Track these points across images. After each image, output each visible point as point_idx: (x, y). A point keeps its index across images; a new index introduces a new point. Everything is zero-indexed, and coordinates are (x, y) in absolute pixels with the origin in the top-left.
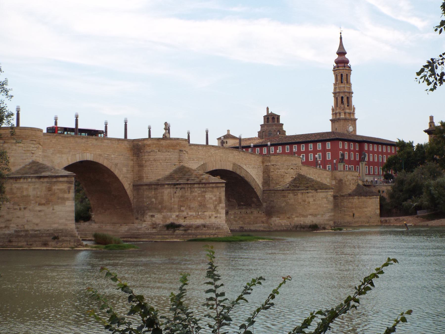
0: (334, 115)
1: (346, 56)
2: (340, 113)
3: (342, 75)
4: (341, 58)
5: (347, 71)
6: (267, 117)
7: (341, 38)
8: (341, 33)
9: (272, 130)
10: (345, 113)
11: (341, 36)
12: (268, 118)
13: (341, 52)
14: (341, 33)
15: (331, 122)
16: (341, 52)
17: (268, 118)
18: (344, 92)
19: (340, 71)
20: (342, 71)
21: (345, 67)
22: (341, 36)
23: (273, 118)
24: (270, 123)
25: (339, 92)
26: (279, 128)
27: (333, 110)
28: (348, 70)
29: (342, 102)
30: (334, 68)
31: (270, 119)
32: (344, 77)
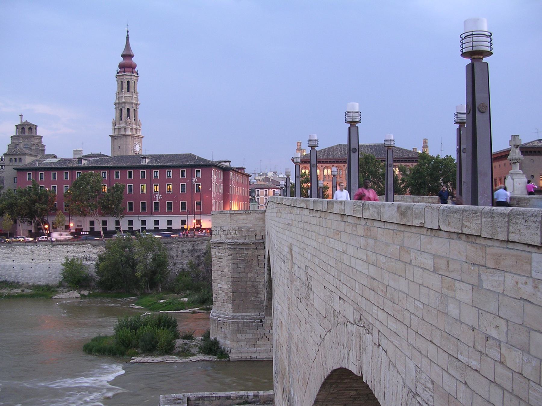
0: (117, 130)
1: (134, 60)
2: (125, 128)
3: (128, 82)
4: (127, 61)
5: (135, 78)
6: (21, 127)
7: (128, 38)
8: (128, 32)
9: (29, 144)
10: (132, 129)
11: (128, 35)
12: (23, 128)
13: (127, 55)
14: (128, 32)
15: (110, 138)
16: (127, 55)
17: (23, 128)
18: (132, 103)
19: (127, 77)
20: (129, 77)
21: (133, 73)
22: (128, 35)
23: (30, 129)
24: (27, 134)
25: (125, 103)
26: (37, 141)
27: (114, 124)
28: (136, 76)
29: (128, 115)
30: (118, 73)
31: (27, 130)
32: (131, 85)
